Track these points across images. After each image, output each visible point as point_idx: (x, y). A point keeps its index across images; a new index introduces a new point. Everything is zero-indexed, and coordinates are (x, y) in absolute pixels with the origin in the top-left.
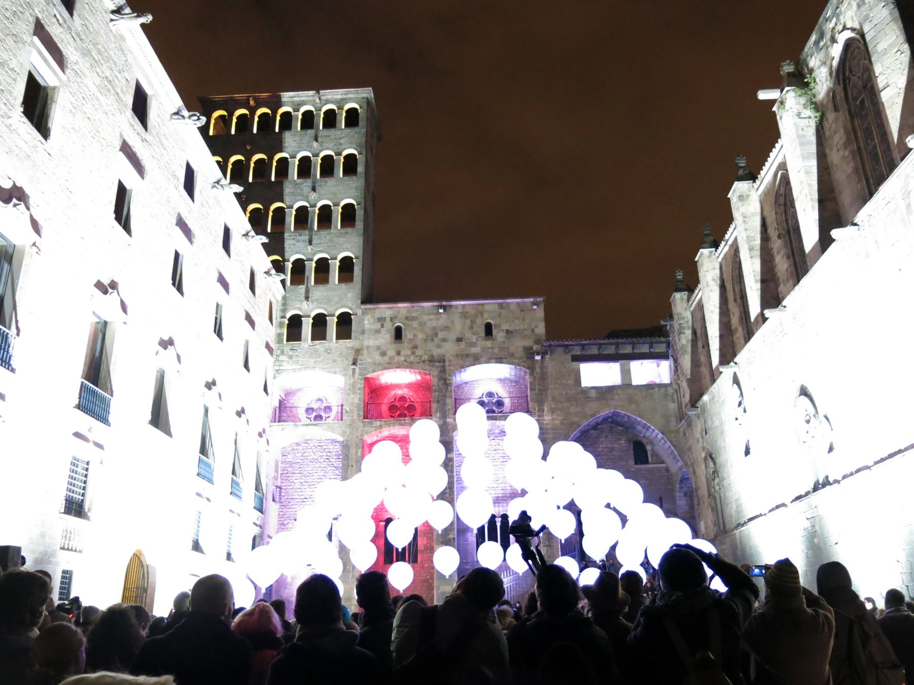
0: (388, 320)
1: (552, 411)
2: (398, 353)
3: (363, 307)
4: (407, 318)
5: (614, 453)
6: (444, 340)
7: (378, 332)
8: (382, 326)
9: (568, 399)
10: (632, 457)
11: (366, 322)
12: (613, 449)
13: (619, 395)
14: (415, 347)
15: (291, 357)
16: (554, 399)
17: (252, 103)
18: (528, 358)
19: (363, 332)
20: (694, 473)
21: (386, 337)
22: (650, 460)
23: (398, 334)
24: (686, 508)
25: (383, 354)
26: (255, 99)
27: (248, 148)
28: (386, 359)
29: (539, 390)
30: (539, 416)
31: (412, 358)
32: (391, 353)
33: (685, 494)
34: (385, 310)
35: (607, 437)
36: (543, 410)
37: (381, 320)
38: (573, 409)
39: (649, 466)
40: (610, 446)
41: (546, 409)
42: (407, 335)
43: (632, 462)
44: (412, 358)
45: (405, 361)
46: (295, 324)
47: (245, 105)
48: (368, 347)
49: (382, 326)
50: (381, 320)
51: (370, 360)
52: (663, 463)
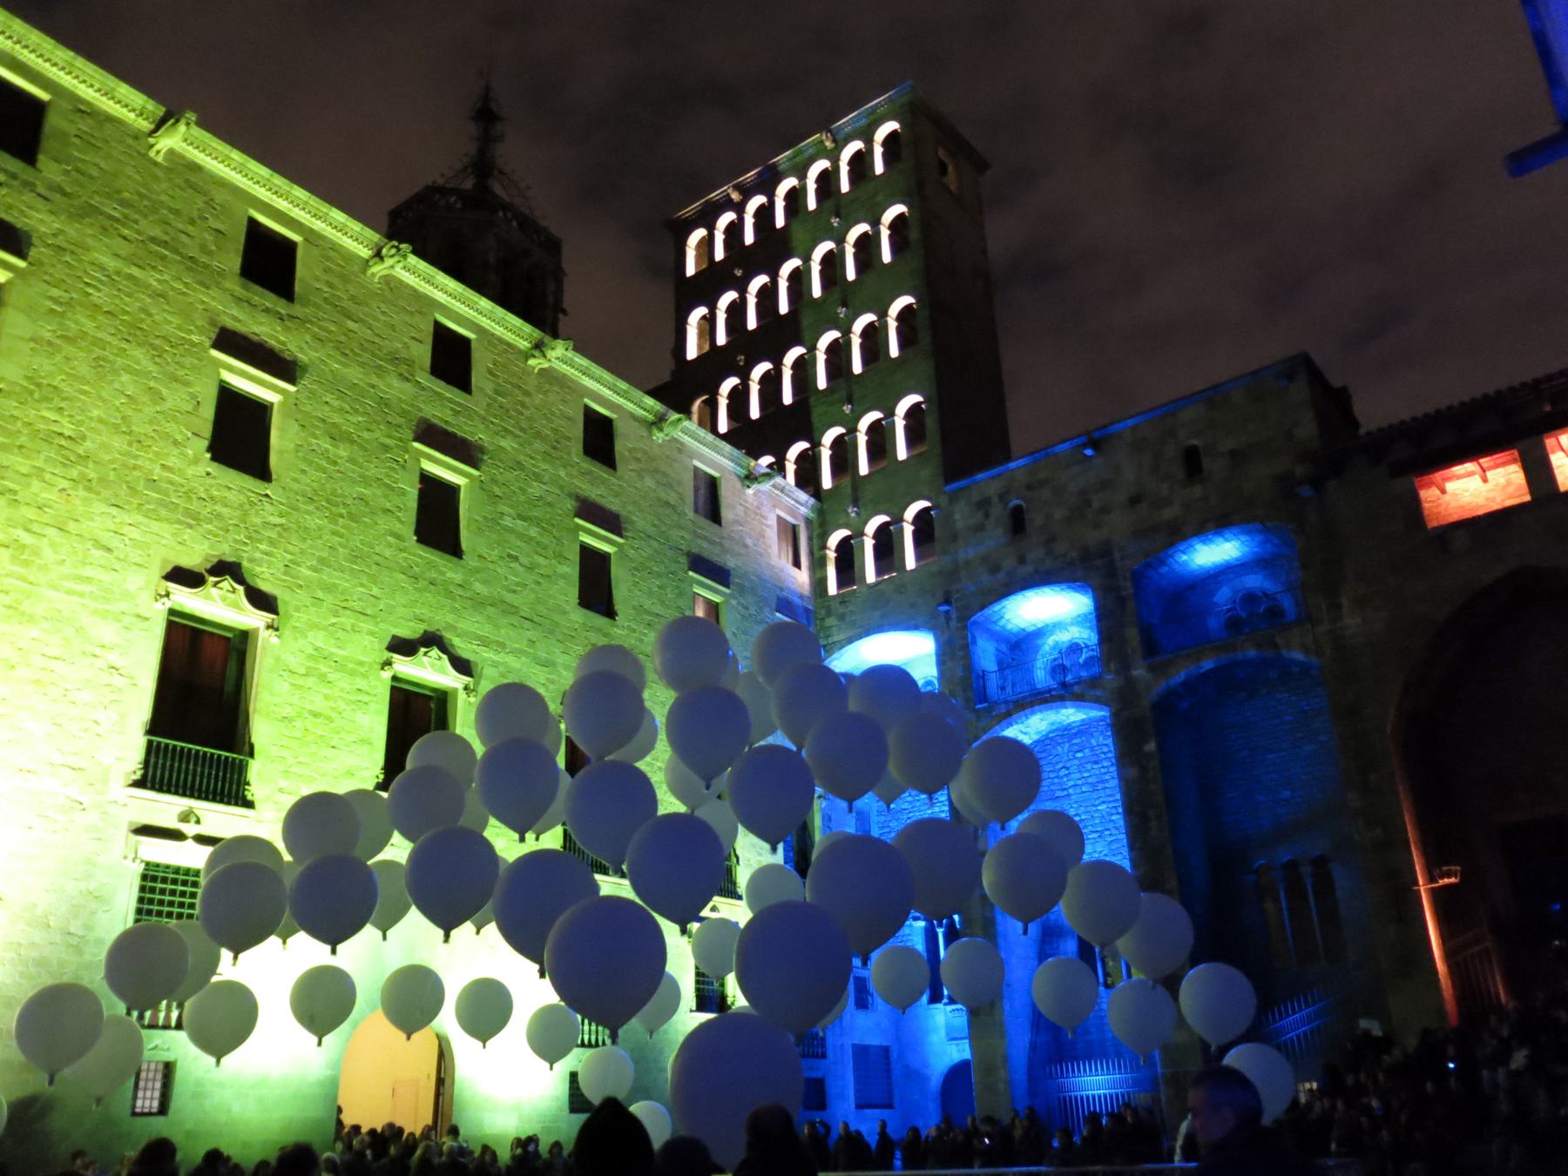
0: (995, 500)
2: (1022, 560)
3: (947, 488)
4: (1029, 487)
6: (1105, 510)
7: (980, 528)
8: (987, 516)
11: (957, 516)
14: (1052, 539)
15: (842, 618)
17: (735, 196)
19: (954, 537)
21: (996, 536)
23: (1017, 522)
25: (995, 569)
26: (737, 188)
27: (739, 273)
28: (1001, 576)
31: (1048, 564)
32: (1009, 563)
34: (987, 482)
37: (983, 504)
42: (1035, 520)
44: (1048, 564)
45: (1036, 571)
46: (847, 557)
47: (727, 204)
48: (967, 563)
49: (987, 516)
50: (983, 504)
51: (973, 588)
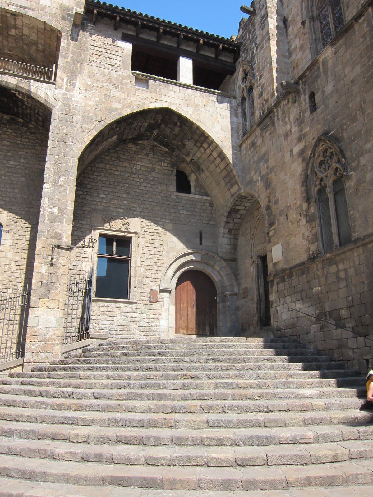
1: (88, 88)
5: (154, 174)
9: (109, 81)
10: (174, 183)
12: (153, 170)
13: (175, 92)
16: (91, 76)
18: (63, 18)
20: (268, 185)
22: (193, 190)
24: (228, 247)
29: (72, 60)
30: (67, 90)
33: (230, 230)
35: (147, 154)
36: (74, 85)
38: (115, 92)
39: (192, 196)
40: (150, 165)
41: (78, 83)
43: (173, 188)
52: (206, 195)
